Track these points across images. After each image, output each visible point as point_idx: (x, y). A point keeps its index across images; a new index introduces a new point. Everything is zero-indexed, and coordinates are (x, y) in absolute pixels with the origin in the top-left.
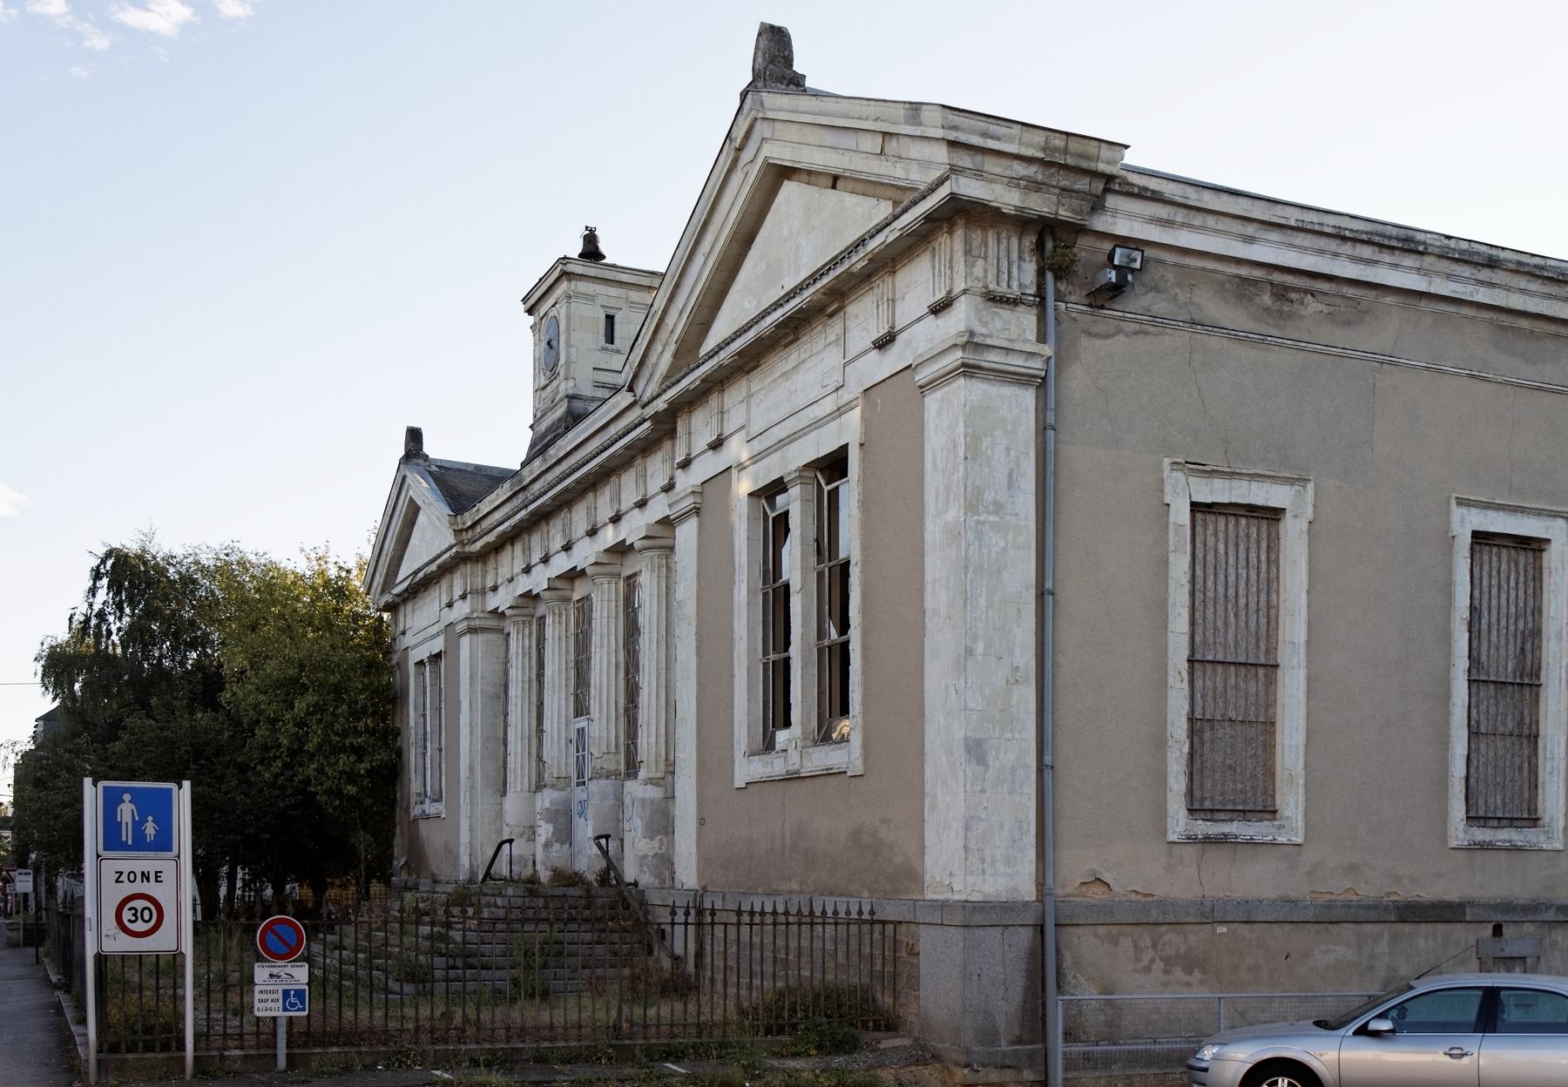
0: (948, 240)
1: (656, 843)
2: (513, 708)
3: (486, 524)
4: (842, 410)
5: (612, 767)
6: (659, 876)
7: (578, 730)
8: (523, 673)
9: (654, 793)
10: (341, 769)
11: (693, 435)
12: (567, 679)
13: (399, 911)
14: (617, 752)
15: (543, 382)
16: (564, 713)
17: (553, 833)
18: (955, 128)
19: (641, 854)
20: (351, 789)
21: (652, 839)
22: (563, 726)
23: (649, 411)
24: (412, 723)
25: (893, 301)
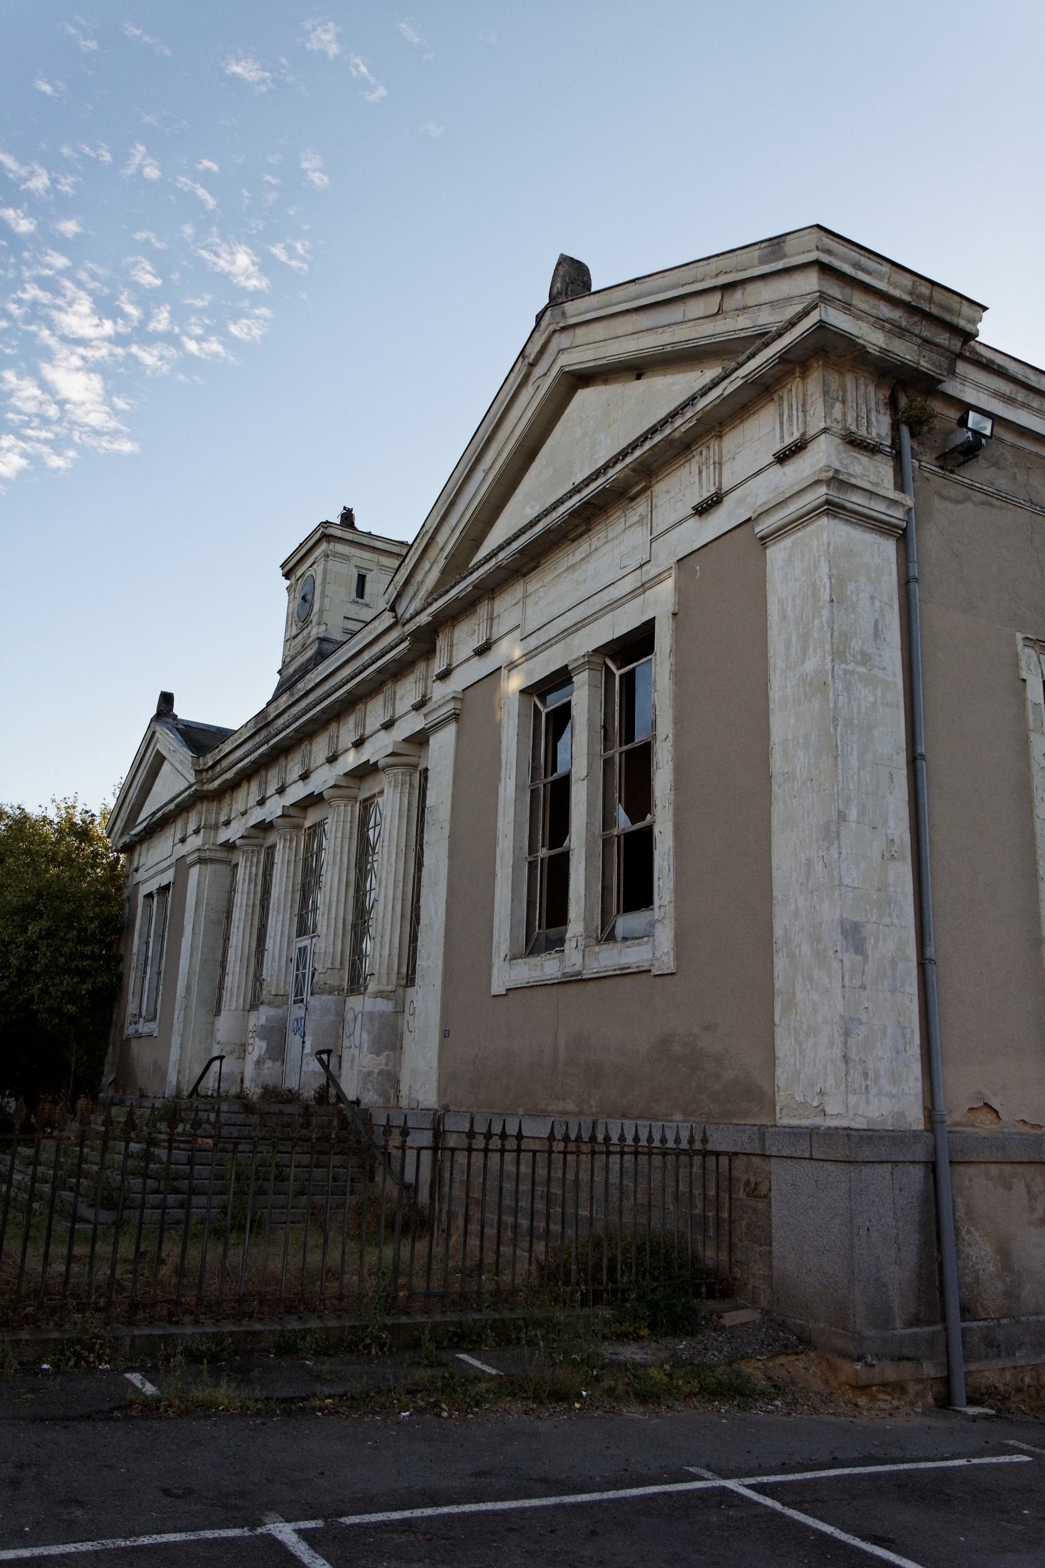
0: (800, 385)
1: (382, 1059)
2: (236, 931)
3: (225, 763)
4: (647, 586)
5: (336, 983)
6: (384, 1095)
7: (300, 949)
8: (248, 898)
9: (384, 1006)
10: (64, 989)
11: (455, 647)
12: (292, 900)
14: (342, 968)
15: (294, 632)
16: (286, 932)
17: (267, 1050)
18: (829, 252)
19: (365, 1070)
20: (71, 1008)
21: (378, 1055)
22: (285, 945)
23: (411, 627)
24: (135, 950)
25: (720, 464)
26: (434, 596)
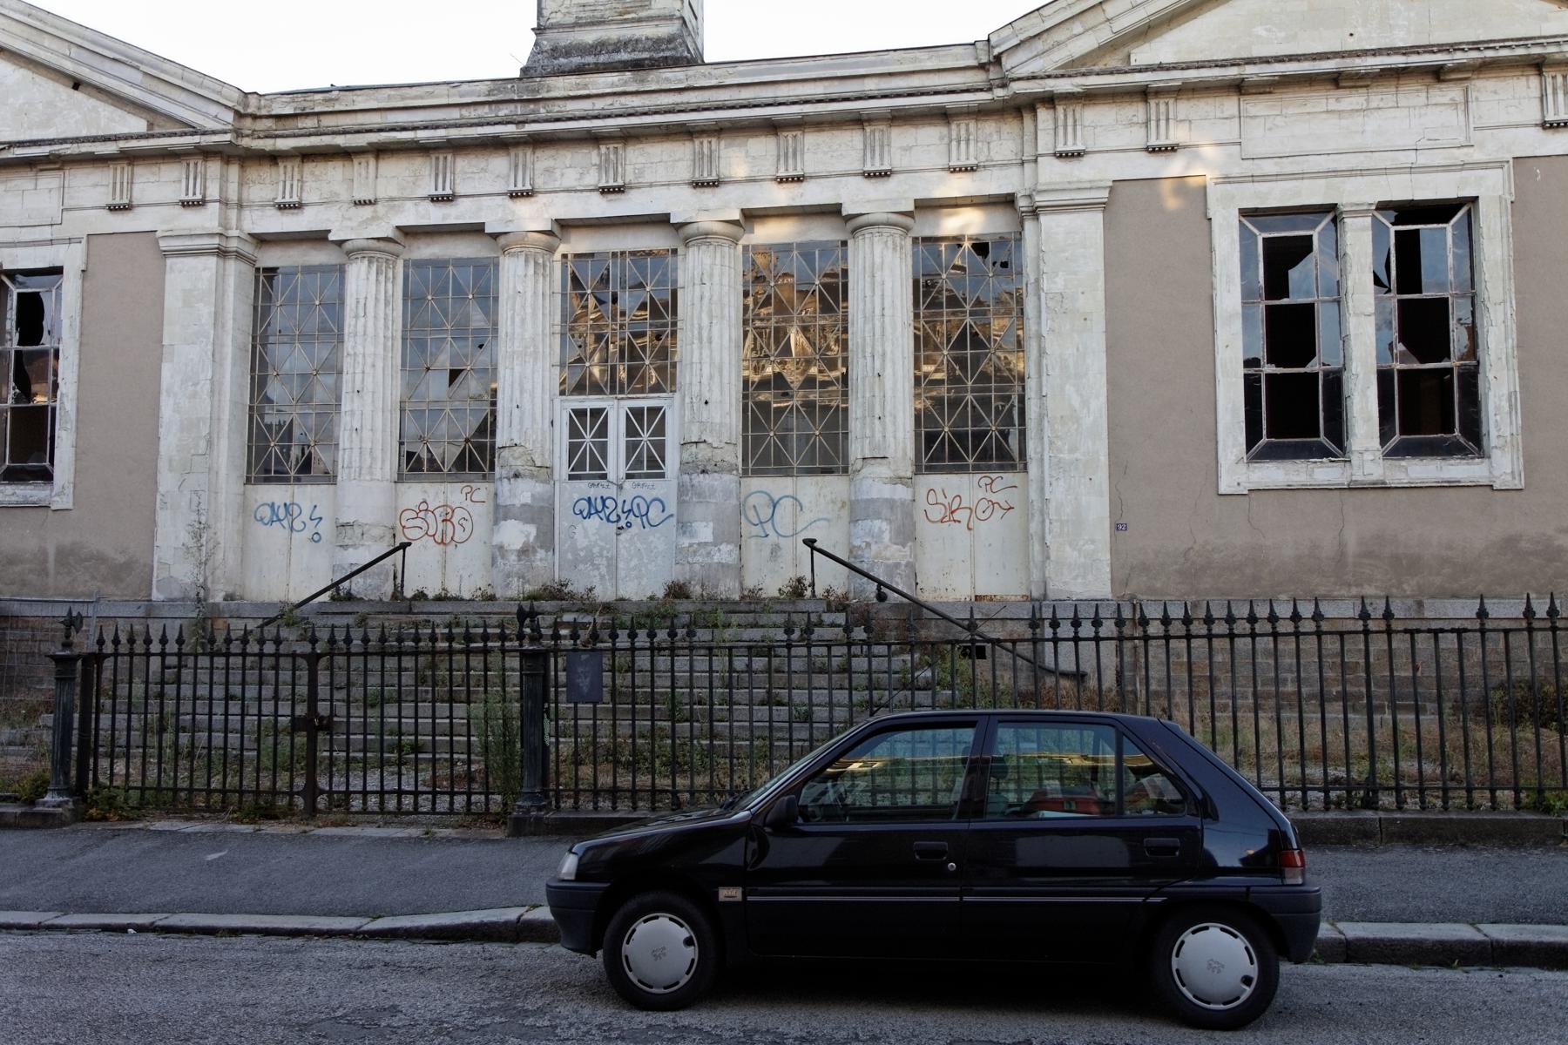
3: (328, 121)
13: (397, 640)
17: (537, 537)
26: (1071, 71)
